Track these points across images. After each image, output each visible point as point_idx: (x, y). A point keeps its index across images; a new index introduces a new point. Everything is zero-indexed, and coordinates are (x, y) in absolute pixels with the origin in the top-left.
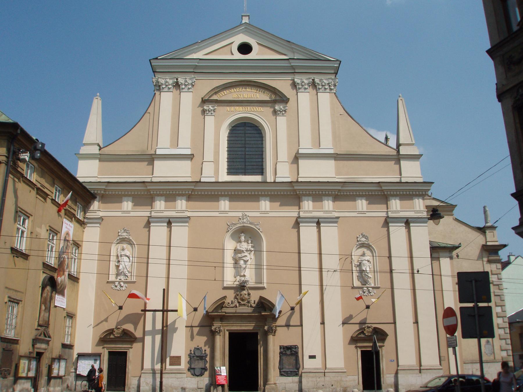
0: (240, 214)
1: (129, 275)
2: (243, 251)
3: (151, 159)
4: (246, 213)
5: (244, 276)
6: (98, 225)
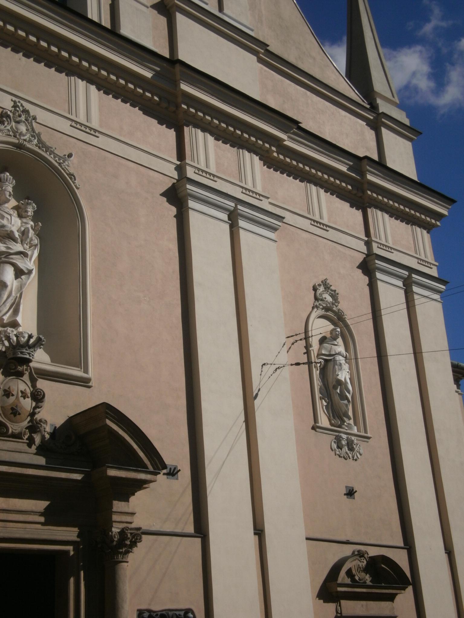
2: (10, 237)
4: (27, 106)
5: (15, 324)
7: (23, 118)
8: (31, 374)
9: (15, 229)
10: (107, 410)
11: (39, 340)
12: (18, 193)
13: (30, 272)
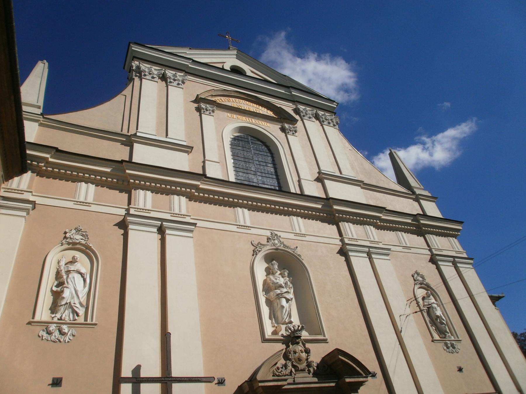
0: (268, 234)
1: (81, 311)
2: (281, 286)
3: (129, 141)
4: (276, 233)
5: (291, 322)
6: (24, 214)
7: (276, 238)
8: (302, 342)
9: (282, 283)
10: (338, 352)
11: (302, 327)
12: (280, 268)
13: (292, 299)
